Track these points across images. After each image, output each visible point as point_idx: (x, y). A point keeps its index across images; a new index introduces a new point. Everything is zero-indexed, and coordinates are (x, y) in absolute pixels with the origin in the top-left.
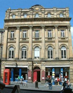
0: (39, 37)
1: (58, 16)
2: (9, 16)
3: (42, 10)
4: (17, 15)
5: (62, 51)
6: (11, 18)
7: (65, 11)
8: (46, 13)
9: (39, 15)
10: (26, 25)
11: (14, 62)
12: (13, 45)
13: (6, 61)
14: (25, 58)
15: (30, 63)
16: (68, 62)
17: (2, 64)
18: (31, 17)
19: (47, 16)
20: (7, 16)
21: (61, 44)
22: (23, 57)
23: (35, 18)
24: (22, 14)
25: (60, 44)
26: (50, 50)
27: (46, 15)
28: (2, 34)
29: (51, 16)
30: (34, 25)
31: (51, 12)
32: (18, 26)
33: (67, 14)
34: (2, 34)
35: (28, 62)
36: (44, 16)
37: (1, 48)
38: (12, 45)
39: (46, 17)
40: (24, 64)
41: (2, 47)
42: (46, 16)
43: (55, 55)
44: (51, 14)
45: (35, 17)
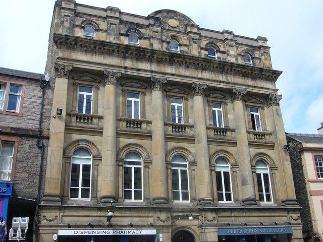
2: (74, 26)
4: (102, 30)
6: (80, 33)
9: (180, 45)
10: (142, 74)
12: (88, 141)
13: (61, 208)
15: (163, 216)
16: (284, 213)
17: (44, 222)
18: (154, 45)
20: (62, 23)
27: (202, 49)
30: (170, 78)
31: (219, 45)
32: (111, 70)
33: (266, 59)
35: (158, 214)
36: (200, 53)
37: (40, 151)
39: (203, 56)
40: (140, 223)
41: (42, 148)
43: (239, 187)
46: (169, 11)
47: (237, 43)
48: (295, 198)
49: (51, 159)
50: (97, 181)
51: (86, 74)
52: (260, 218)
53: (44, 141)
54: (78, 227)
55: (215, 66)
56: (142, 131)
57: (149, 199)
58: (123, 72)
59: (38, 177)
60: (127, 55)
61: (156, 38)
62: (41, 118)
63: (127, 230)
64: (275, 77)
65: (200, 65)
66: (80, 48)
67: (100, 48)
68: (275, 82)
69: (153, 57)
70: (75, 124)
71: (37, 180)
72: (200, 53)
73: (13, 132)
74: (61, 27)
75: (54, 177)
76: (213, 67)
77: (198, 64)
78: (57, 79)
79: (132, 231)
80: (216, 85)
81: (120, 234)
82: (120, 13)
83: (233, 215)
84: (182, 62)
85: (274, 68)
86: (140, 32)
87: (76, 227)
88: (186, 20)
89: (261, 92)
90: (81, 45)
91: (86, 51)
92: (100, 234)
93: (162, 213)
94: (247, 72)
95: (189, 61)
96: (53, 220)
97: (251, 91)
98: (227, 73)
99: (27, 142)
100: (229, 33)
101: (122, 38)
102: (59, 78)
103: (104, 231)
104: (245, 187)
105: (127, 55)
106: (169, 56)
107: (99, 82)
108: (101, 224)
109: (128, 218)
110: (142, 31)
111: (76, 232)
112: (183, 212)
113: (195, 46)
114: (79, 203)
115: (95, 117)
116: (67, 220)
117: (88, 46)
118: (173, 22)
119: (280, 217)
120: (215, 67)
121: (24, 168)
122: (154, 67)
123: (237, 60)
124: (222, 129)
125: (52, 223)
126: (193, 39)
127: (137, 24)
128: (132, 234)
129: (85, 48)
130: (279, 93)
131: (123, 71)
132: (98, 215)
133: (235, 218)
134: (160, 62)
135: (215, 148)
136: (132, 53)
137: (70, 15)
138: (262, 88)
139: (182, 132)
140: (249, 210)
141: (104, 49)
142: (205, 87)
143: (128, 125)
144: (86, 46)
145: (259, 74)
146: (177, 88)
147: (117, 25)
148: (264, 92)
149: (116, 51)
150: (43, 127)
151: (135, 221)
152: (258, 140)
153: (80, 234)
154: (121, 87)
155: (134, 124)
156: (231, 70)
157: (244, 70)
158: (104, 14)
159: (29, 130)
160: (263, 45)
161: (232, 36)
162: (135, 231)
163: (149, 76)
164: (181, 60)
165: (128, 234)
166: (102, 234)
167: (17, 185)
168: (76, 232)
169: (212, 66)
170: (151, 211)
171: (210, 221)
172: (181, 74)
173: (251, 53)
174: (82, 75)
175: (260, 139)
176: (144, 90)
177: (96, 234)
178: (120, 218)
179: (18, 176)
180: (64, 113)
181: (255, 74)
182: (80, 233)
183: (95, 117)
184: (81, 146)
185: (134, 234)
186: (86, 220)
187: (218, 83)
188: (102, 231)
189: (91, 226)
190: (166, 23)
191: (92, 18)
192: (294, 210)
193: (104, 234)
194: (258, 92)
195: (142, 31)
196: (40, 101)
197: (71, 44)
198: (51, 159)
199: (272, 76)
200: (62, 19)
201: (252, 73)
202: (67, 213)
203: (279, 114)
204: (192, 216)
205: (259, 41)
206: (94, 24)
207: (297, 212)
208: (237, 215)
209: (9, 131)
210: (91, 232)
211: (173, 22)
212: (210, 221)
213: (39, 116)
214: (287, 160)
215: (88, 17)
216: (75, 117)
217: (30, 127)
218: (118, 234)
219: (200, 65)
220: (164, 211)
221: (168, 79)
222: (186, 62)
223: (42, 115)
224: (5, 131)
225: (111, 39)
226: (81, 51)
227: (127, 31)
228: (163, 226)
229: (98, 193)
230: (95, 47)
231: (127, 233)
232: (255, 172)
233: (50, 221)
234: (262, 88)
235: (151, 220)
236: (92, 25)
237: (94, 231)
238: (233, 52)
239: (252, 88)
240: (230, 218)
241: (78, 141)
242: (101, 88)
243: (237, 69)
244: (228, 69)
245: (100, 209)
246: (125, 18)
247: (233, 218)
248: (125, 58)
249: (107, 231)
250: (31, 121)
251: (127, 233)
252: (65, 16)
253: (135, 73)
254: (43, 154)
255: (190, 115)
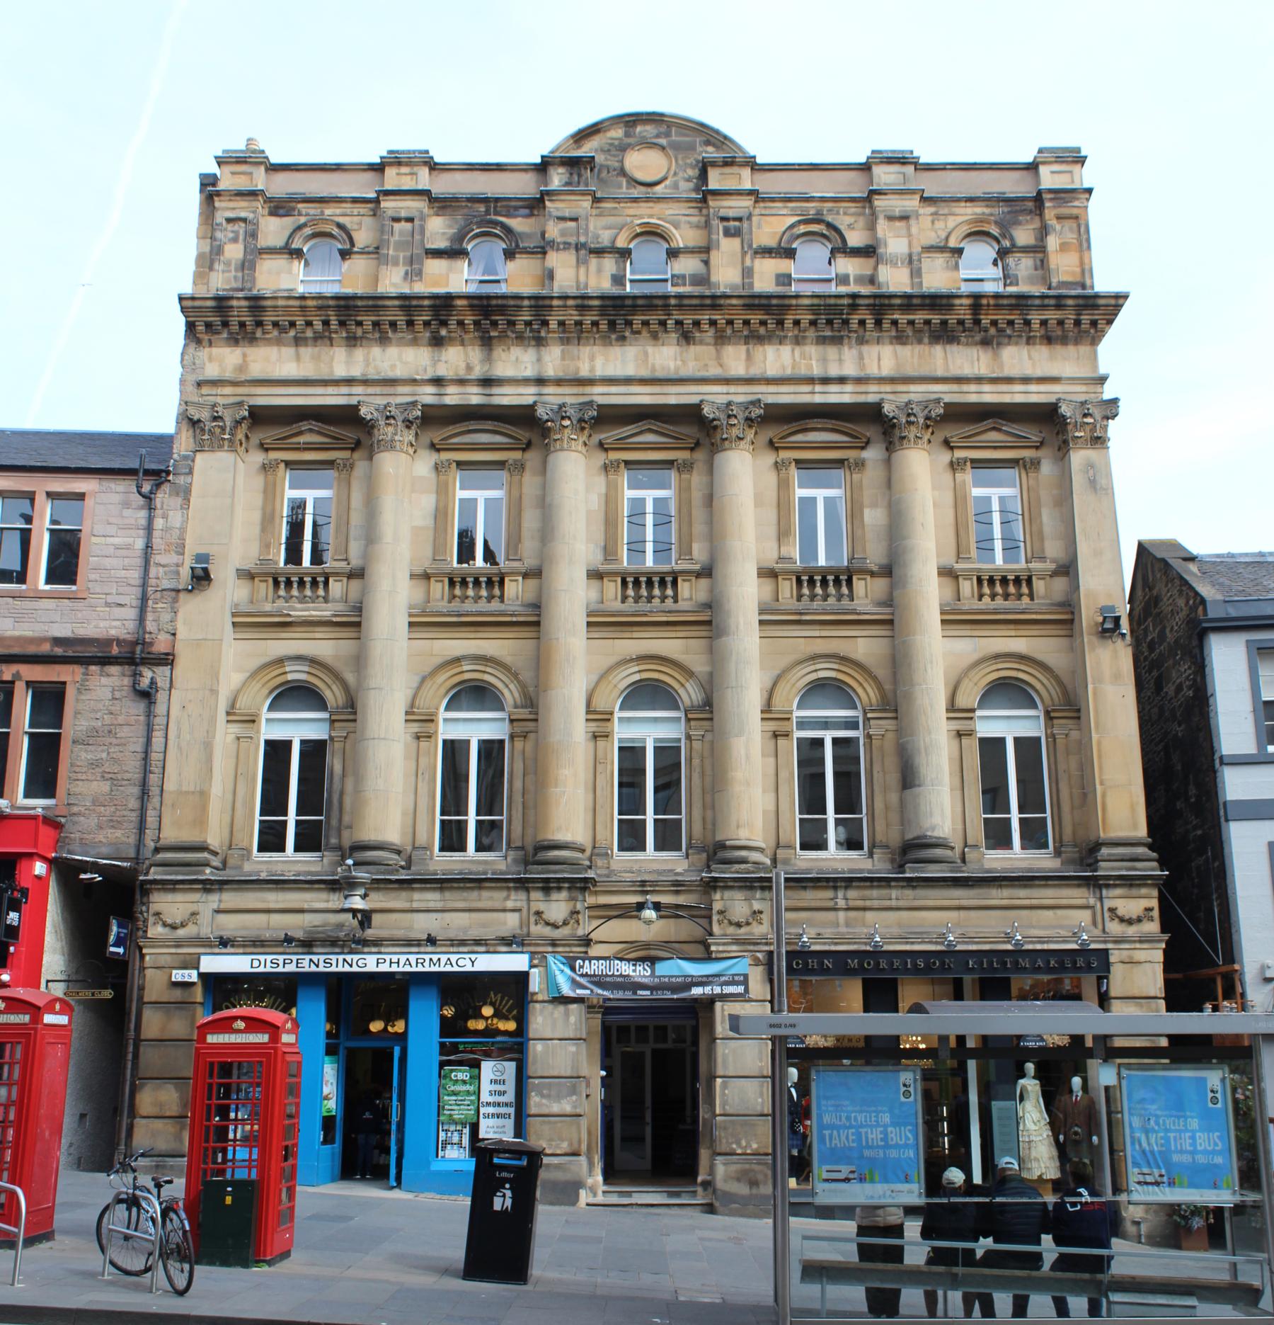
0: (675, 564)
1: (936, 278)
2: (256, 253)
3: (715, 181)
5: (993, 748)
7: (1038, 199)
8: (769, 229)
9: (673, 253)
10: (507, 397)
11: (335, 901)
12: (313, 661)
13: (208, 886)
14: (489, 836)
15: (557, 907)
17: (155, 931)
19: (785, 279)
20: (217, 251)
21: (976, 656)
22: (462, 826)
23: (616, 291)
24: (438, 229)
25: (969, 647)
26: (828, 736)
27: (767, 252)
28: (149, 498)
29: (843, 280)
31: (842, 222)
34: (149, 498)
35: (537, 900)
36: (747, 273)
37: (139, 707)
38: (299, 658)
41: (146, 696)
42: (765, 276)
44: (842, 249)
45: (618, 280)
46: (631, 120)
47: (925, 200)
48: (1142, 831)
49: (179, 729)
50: (342, 794)
51: (305, 426)
52: (963, 913)
53: (162, 673)
54: (263, 946)
55: (806, 318)
56: (502, 607)
57: (522, 848)
58: (429, 400)
59: (136, 791)
60: (443, 332)
61: (567, 246)
62: (144, 599)
63: (427, 957)
64: (1094, 323)
65: (738, 324)
66: (275, 333)
67: (342, 324)
68: (1095, 341)
69: (545, 323)
70: (268, 607)
71: (134, 803)
72: (747, 273)
73: (59, 651)
74: (216, 266)
75: (192, 789)
76: (797, 323)
77: (730, 322)
78: (199, 456)
79: (444, 958)
80: (807, 399)
81: (401, 969)
82: (433, 166)
83: (841, 903)
84: (663, 324)
85: (1103, 283)
86: (508, 230)
87: (255, 946)
88: (708, 143)
89: (1019, 399)
90: (275, 324)
91: (298, 341)
92: (334, 969)
93: (555, 896)
94: (952, 319)
95: (688, 319)
96: (183, 925)
97: (973, 398)
98: (862, 341)
99: (104, 680)
100: (900, 160)
101: (434, 267)
102: (206, 455)
103: (348, 958)
104: (908, 792)
105: (443, 332)
106: (603, 310)
107: (357, 446)
108: (342, 934)
109: (434, 915)
110: (517, 224)
111: (256, 963)
112: (647, 892)
113: (728, 248)
114: (279, 868)
115: (336, 574)
116: (231, 925)
117: (300, 322)
118: (644, 163)
119: (1059, 912)
120: (804, 324)
121: (95, 764)
122: (553, 360)
123: (916, 273)
124: (824, 573)
125: (181, 933)
126: (724, 219)
127: (497, 200)
128: (442, 969)
129: (292, 333)
130: (1107, 395)
131: (428, 395)
132: (331, 905)
133: (852, 914)
134: (574, 334)
135: (802, 642)
136: (461, 323)
137: (243, 214)
138: (1026, 380)
139: (663, 598)
140: (912, 883)
141: (360, 324)
142: (758, 412)
143: (458, 591)
144: (292, 324)
145: (1011, 323)
146: (650, 431)
147: (417, 222)
148: (1034, 399)
149: (402, 324)
150: (150, 626)
151: (459, 923)
152: (999, 601)
153: (268, 969)
154: (435, 457)
155: (477, 583)
156: (878, 323)
157: (936, 318)
158: (364, 187)
159: (108, 642)
160: (1060, 182)
161: (911, 169)
162: (454, 958)
163: (529, 400)
164: (653, 318)
165: (427, 969)
166: (340, 969)
167: (75, 819)
168: (256, 963)
169: (788, 324)
170: (516, 889)
171: (739, 925)
172: (660, 374)
173: (995, 231)
174: (295, 428)
175: (1006, 596)
176: (517, 455)
177: (321, 969)
178: (409, 915)
179: (77, 790)
180: (223, 573)
181: (994, 323)
182: (268, 963)
183: (336, 574)
184: (290, 677)
185: (448, 969)
186: (297, 925)
187: (818, 388)
188: (341, 957)
189: (307, 945)
190: (622, 172)
191: (328, 212)
192: (1129, 882)
193: (347, 969)
194: (1007, 399)
195: (517, 224)
196: (140, 544)
197: (242, 325)
198: (179, 729)
199: (1077, 323)
200: (219, 235)
201: (977, 322)
202: (230, 899)
203: (1100, 485)
204: (657, 906)
205: (1044, 170)
206: (336, 231)
207: (1144, 891)
208: (860, 903)
209: (46, 648)
210: (306, 963)
211: (644, 163)
212: (739, 925)
213: (137, 592)
214: (1117, 677)
215: (312, 209)
216: (271, 580)
217: (113, 632)
218: (394, 968)
219: (738, 324)
220: (559, 889)
221: (601, 400)
222: (679, 323)
223: (144, 585)
224: (32, 650)
225: (393, 282)
226: (279, 342)
227: (460, 237)
228: (554, 943)
229: (346, 834)
230: (326, 323)
231: (426, 964)
232: (970, 733)
233: (174, 927)
234: (1026, 380)
235: (511, 922)
236: (330, 235)
237: (315, 958)
238: (895, 243)
239: (973, 387)
240: (830, 915)
241: (280, 661)
242: (361, 467)
243: (902, 318)
244: (862, 323)
245: (334, 886)
246: (443, 185)
247: (841, 914)
248: (437, 342)
249: (356, 957)
250: (117, 610)
251: (426, 964)
252: (229, 220)
253: (474, 396)
254: (149, 714)
255: (699, 528)
